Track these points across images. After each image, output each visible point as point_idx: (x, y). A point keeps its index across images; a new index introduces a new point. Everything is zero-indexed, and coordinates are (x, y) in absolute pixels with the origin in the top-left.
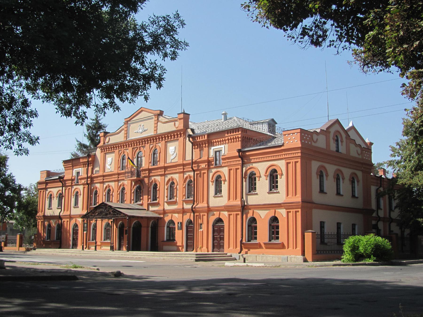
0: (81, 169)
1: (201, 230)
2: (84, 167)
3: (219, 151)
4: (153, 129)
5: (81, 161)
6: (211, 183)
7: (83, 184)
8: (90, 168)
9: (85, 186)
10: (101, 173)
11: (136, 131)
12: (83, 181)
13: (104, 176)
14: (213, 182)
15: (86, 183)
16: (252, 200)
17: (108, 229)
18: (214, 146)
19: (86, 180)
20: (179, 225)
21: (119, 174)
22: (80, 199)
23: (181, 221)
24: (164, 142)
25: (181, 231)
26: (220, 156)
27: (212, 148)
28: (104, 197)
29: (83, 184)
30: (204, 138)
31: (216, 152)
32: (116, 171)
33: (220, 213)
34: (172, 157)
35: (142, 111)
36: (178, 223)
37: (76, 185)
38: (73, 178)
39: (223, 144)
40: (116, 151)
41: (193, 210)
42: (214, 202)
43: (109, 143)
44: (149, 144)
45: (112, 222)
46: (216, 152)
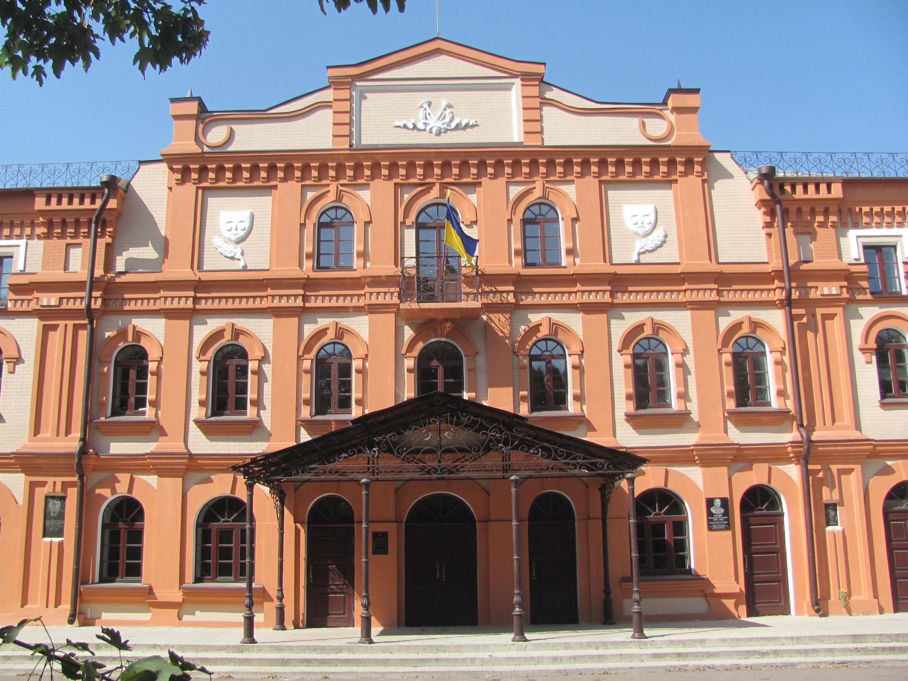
0: (22, 242)
1: (838, 528)
3: (878, 249)
5: (40, 203)
6: (859, 358)
7: (43, 314)
10: (178, 269)
11: (398, 124)
13: (199, 286)
14: (863, 350)
18: (856, 226)
20: (717, 510)
21: (308, 284)
23: (727, 495)
24: (591, 182)
25: (729, 533)
27: (852, 233)
29: (43, 314)
30: (829, 191)
32: (291, 270)
34: (640, 244)
35: (438, 52)
36: (710, 502)
43: (231, 148)
44: (502, 180)
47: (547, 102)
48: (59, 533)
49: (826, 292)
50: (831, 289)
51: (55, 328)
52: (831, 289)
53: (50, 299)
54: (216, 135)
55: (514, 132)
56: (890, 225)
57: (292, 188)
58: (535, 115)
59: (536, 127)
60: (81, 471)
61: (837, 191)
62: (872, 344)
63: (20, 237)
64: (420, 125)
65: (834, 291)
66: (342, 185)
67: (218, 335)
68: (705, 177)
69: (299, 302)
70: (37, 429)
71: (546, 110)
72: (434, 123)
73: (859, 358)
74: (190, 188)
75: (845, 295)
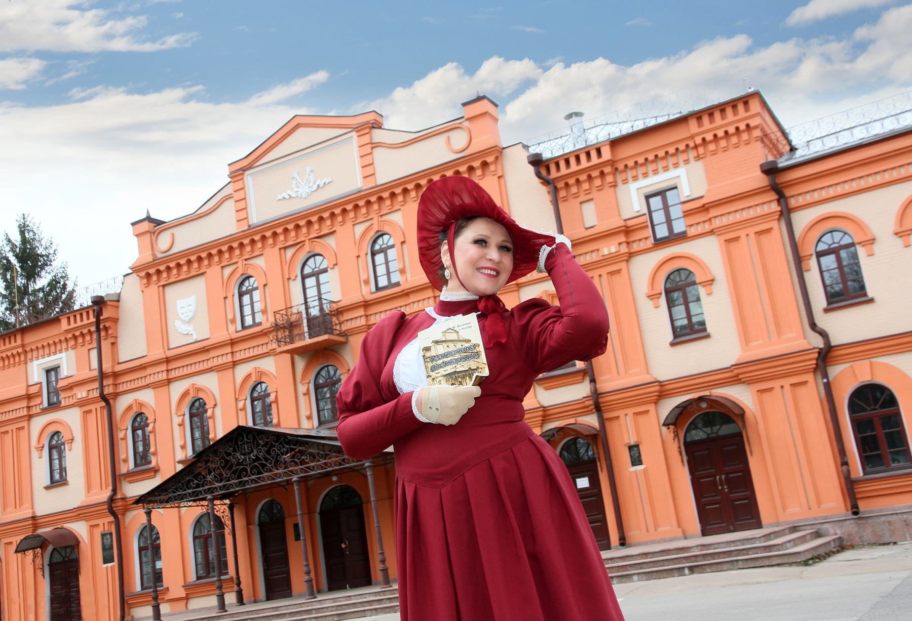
0: (63, 355)
2: (74, 347)
3: (662, 193)
4: (358, 173)
7: (81, 404)
8: (105, 345)
9: (92, 407)
11: (280, 197)
12: (81, 393)
13: (168, 360)
15: (96, 394)
16: (845, 326)
17: (209, 537)
18: (635, 178)
19: (96, 385)
21: (233, 343)
22: (74, 459)
26: (666, 208)
28: (177, 429)
29: (81, 404)
31: (648, 197)
33: (871, 362)
35: (298, 126)
37: (44, 411)
38: (33, 390)
39: (676, 165)
40: (209, 271)
41: (597, 403)
42: (672, 363)
43: (175, 250)
44: (349, 224)
45: (231, 508)
46: (648, 197)
47: (375, 145)
48: (112, 560)
49: (606, 251)
50: (610, 248)
51: (90, 411)
52: (610, 248)
53: (81, 393)
54: (163, 242)
55: (351, 181)
56: (666, 169)
57: (214, 271)
58: (368, 160)
59: (369, 171)
60: (112, 512)
61: (606, 154)
62: (661, 287)
63: (61, 351)
64: (293, 195)
65: (613, 249)
66: (246, 260)
67: (185, 394)
68: (500, 174)
69: (229, 358)
70: (89, 488)
71: (377, 152)
72: (304, 190)
73: (646, 306)
74: (154, 288)
75: (624, 249)
